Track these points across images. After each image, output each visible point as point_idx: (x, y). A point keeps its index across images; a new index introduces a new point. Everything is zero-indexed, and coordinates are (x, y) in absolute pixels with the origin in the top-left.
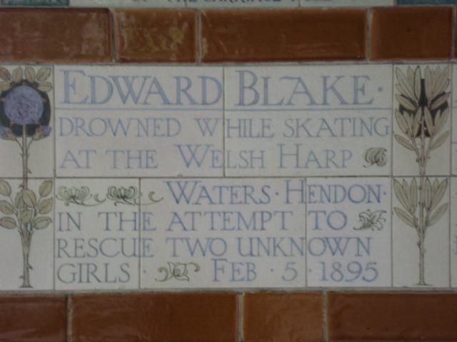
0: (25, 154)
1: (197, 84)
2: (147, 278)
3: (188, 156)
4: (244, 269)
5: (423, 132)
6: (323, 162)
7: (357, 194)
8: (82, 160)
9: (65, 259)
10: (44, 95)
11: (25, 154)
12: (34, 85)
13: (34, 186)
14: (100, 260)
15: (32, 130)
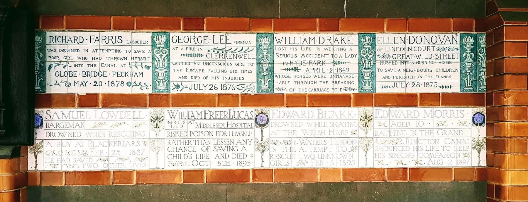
0: (262, 131)
1: (307, 113)
2: (294, 165)
3: (305, 132)
4: (319, 162)
5: (366, 126)
6: (340, 134)
7: (349, 142)
8: (276, 133)
9: (272, 159)
10: (267, 116)
11: (262, 131)
12: (265, 114)
13: (264, 140)
14: (281, 160)
15: (264, 125)
